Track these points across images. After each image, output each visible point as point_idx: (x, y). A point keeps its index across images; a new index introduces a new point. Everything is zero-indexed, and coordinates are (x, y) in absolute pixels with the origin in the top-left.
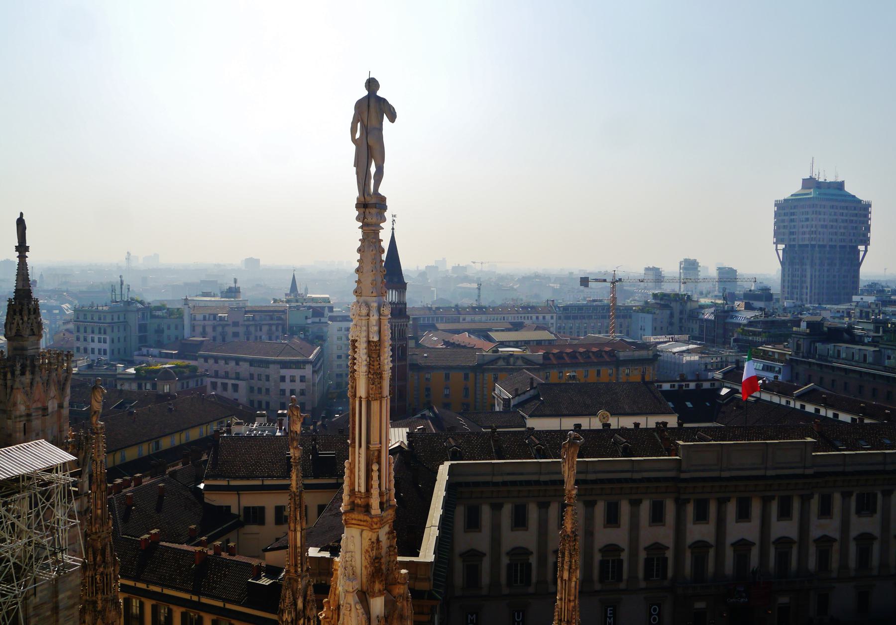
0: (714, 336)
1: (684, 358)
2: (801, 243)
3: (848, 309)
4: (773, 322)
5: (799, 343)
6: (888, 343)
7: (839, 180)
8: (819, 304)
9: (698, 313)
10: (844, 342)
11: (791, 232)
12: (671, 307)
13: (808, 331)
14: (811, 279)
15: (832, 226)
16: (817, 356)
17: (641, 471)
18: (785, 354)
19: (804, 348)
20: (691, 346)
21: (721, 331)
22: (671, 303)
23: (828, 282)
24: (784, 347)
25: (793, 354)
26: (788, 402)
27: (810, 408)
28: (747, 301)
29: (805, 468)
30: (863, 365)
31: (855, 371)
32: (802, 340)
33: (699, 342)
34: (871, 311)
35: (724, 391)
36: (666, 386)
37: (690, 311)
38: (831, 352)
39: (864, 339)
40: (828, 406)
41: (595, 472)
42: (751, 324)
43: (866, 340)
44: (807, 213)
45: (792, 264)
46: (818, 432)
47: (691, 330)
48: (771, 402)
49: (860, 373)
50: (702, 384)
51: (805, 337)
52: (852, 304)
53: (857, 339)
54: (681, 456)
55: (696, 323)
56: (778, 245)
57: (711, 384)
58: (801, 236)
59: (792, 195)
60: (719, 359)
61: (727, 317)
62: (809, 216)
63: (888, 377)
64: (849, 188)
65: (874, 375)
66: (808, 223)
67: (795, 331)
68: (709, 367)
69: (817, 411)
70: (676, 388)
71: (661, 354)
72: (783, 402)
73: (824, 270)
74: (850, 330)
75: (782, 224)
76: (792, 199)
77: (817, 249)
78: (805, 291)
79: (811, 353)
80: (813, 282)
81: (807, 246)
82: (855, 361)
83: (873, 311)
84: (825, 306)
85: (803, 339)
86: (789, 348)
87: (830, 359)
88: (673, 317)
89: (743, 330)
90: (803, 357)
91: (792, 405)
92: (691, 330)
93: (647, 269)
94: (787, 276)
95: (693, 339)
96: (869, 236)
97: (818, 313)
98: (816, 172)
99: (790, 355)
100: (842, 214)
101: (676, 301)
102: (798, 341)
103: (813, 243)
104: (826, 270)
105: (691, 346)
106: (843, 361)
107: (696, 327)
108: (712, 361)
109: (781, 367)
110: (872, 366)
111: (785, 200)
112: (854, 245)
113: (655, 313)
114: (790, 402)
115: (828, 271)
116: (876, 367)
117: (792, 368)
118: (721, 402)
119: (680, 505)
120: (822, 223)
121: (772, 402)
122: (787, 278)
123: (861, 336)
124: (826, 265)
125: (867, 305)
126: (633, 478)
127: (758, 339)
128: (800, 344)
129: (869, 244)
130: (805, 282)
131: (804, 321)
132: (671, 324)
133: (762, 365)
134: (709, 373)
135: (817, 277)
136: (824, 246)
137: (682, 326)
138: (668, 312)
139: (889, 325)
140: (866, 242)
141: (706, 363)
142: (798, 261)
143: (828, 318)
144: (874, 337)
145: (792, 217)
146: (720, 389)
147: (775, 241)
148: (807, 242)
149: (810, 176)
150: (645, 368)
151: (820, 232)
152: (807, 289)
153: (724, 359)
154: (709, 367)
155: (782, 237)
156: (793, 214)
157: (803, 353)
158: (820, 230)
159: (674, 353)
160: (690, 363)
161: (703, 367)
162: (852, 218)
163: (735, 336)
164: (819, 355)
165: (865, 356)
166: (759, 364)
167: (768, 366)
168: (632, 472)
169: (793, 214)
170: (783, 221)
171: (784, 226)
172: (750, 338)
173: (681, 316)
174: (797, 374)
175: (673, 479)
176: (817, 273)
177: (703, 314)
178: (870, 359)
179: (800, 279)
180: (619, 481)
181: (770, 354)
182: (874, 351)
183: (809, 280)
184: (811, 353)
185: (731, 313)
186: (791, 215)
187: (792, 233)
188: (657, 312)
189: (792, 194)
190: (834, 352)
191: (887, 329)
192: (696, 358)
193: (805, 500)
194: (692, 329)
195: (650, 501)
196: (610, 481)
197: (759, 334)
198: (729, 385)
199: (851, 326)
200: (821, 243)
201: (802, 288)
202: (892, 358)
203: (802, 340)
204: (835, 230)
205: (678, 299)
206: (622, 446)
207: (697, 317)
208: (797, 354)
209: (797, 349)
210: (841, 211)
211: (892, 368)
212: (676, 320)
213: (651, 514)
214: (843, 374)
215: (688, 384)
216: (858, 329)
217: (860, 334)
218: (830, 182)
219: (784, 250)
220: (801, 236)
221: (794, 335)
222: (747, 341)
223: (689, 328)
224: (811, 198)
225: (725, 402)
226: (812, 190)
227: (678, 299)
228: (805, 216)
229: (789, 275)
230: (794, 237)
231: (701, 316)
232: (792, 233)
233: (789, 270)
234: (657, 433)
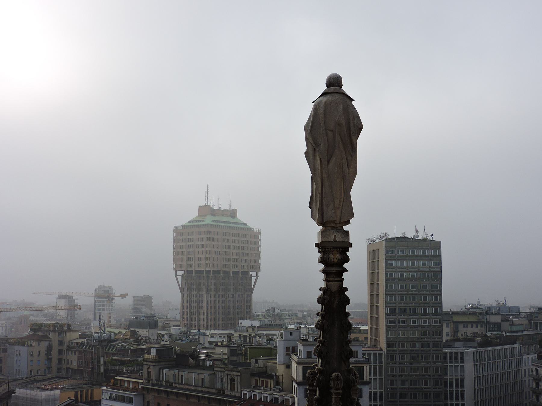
2: (197, 269)
5: (149, 370)
6: (220, 366)
12: (50, 338)
14: (207, 304)
19: (153, 376)
23: (223, 307)
37: (69, 341)
39: (206, 363)
44: (202, 239)
45: (190, 290)
51: (154, 364)
53: (201, 363)
55: (75, 354)
58: (197, 262)
59: (189, 222)
62: (203, 243)
66: (203, 249)
73: (219, 295)
75: (180, 250)
78: (202, 317)
80: (209, 307)
81: (202, 272)
83: (250, 335)
85: (152, 366)
90: (153, 385)
93: (60, 297)
96: (259, 262)
97: (197, 339)
98: (210, 200)
99: (142, 383)
100: (234, 241)
102: (149, 368)
103: (208, 269)
104: (221, 296)
111: (183, 226)
112: (246, 270)
113: (31, 345)
115: (223, 296)
120: (216, 249)
122: (185, 305)
124: (221, 290)
129: (259, 270)
130: (202, 308)
135: (213, 302)
136: (218, 272)
138: (46, 344)
140: (257, 268)
142: (195, 287)
147: (174, 267)
148: (202, 269)
149: (205, 204)
151: (214, 258)
152: (204, 315)
155: (180, 263)
156: (190, 240)
157: (152, 380)
162: (243, 245)
164: (166, 382)
170: (181, 247)
171: (182, 252)
173: (60, 348)
176: (213, 299)
179: (198, 305)
182: (210, 374)
186: (188, 242)
188: (34, 344)
194: (71, 360)
200: (215, 269)
201: (199, 314)
203: (151, 367)
204: (228, 257)
218: (225, 210)
219: (182, 276)
220: (197, 262)
223: (68, 360)
232: (189, 259)
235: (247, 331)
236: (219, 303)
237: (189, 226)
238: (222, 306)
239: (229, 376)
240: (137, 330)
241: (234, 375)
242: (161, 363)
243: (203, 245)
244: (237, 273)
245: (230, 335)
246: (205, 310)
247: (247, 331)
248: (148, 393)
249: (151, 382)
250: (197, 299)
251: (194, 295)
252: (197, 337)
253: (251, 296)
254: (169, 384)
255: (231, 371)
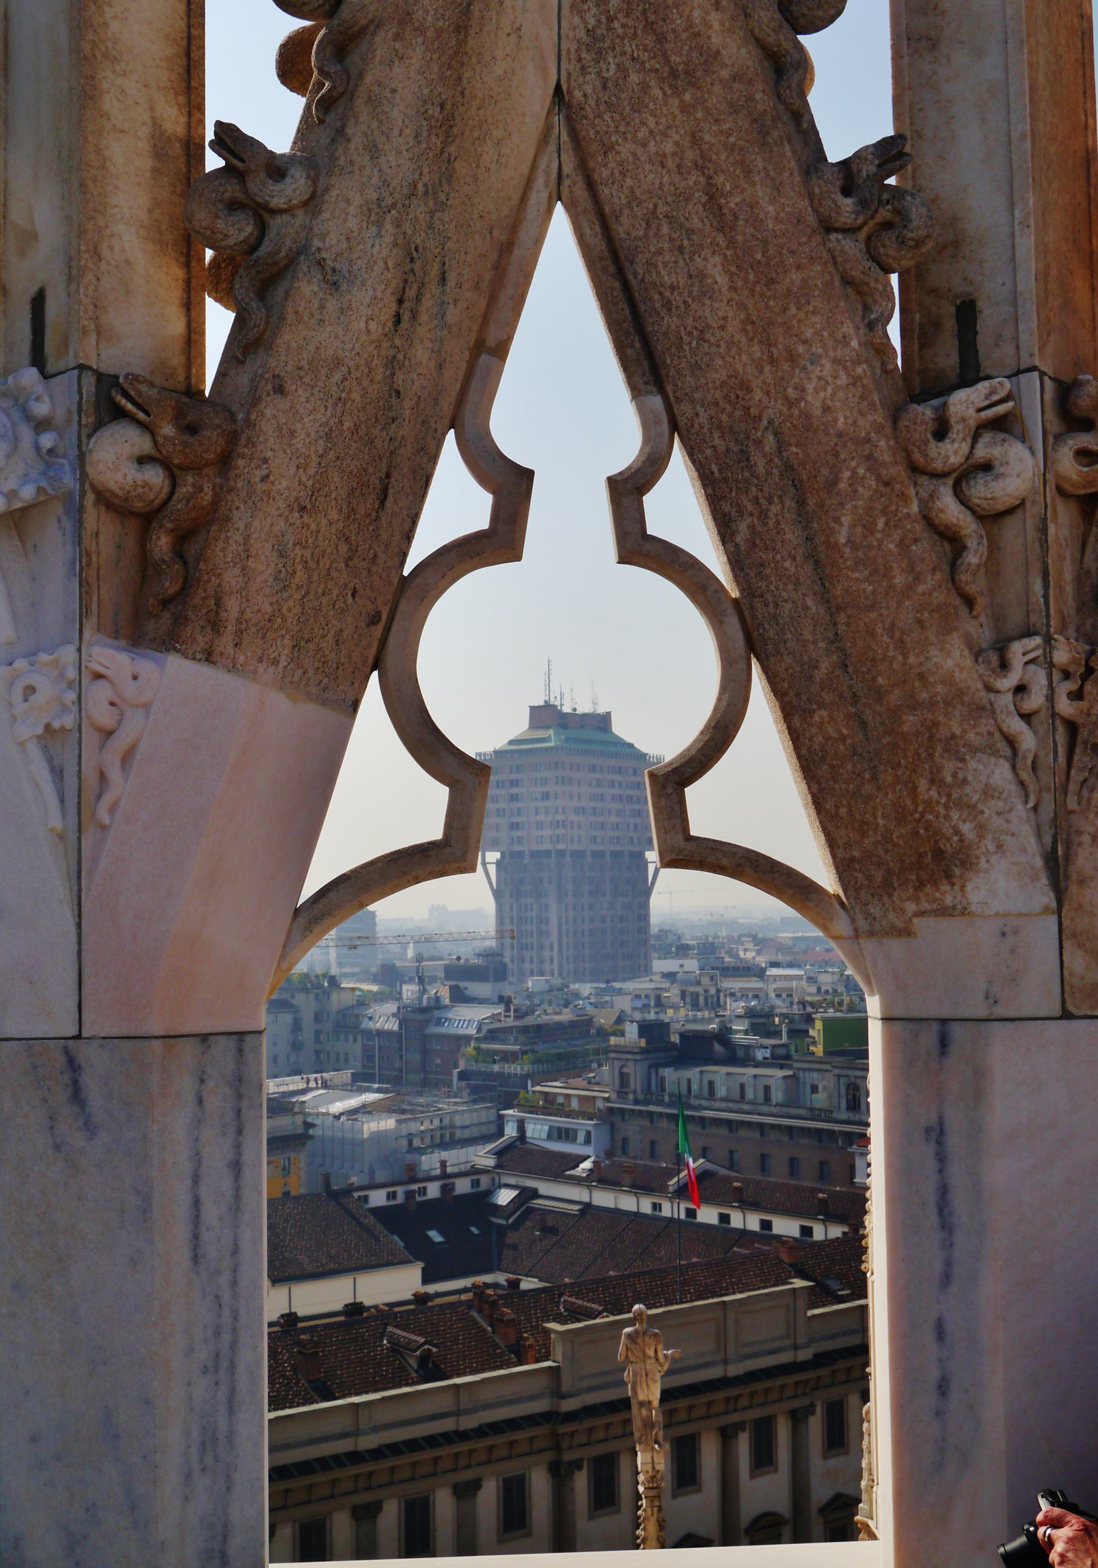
0: (400, 1070)
1: (366, 1127)
2: (535, 848)
3: (657, 989)
4: (539, 1028)
5: (625, 1070)
7: (601, 710)
8: (608, 982)
9: (357, 1016)
10: (716, 1063)
11: (513, 824)
13: (643, 1043)
14: (560, 925)
15: (595, 809)
16: (667, 1098)
17: (475, 1410)
18: (594, 1098)
20: (370, 1097)
21: (415, 1057)
22: (293, 997)
24: (589, 1083)
25: (614, 1096)
26: (656, 1207)
27: (708, 1215)
28: (453, 983)
29: (796, 1347)
30: (765, 1109)
31: (749, 1124)
32: (631, 1064)
33: (376, 1086)
34: (702, 992)
35: (505, 1197)
36: (378, 1198)
37: (338, 1012)
38: (695, 1087)
40: (747, 1204)
41: (375, 1429)
42: (493, 1035)
43: (760, 1055)
45: (517, 894)
46: (791, 1265)
47: (342, 1057)
48: (617, 1212)
49: (761, 1126)
50: (453, 1184)
51: (637, 1057)
52: (653, 978)
53: (740, 1053)
54: (559, 1358)
55: (355, 1040)
56: (487, 853)
57: (472, 1181)
59: (511, 742)
60: (436, 1122)
61: (427, 1021)
62: (549, 789)
63: (819, 1131)
64: (620, 729)
65: (790, 1129)
67: (616, 1046)
68: (417, 1143)
69: (725, 1218)
70: (400, 1199)
71: (316, 1122)
72: (646, 1207)
74: (723, 1036)
76: (512, 752)
77: (568, 859)
78: (547, 954)
79: (653, 1092)
80: (564, 932)
81: (547, 853)
82: (748, 1103)
83: (706, 991)
84: (617, 985)
86: (598, 1084)
87: (697, 1102)
88: (301, 1030)
89: (477, 1049)
90: (636, 1102)
91: (667, 1211)
92: (342, 1057)
94: (507, 920)
95: (360, 1080)
98: (555, 692)
99: (607, 1100)
101: (305, 990)
102: (622, 1066)
103: (560, 847)
105: (370, 1097)
106: (724, 1105)
107: (355, 1049)
108: (422, 1128)
109: (591, 1128)
110: (785, 1110)
111: (496, 752)
112: (636, 849)
114: (660, 1205)
116: (794, 1111)
117: (612, 1126)
118: (503, 1222)
119: (560, 1473)
121: (620, 1210)
122: (508, 927)
123: (747, 1048)
125: (693, 979)
126: (461, 1428)
127: (515, 1069)
128: (628, 1074)
130: (547, 934)
131: (632, 1022)
132: (296, 1046)
133: (546, 1128)
134: (423, 1158)
136: (578, 854)
137: (321, 1052)
139: (777, 1020)
141: (410, 1134)
143: (628, 1011)
144: (774, 1046)
145: (515, 791)
146: (489, 1193)
148: (547, 846)
149: (546, 702)
150: (289, 1159)
153: (446, 1122)
154: (417, 1143)
157: (635, 1092)
158: (573, 818)
159: (337, 1117)
160: (379, 1137)
161: (404, 1143)
162: (630, 792)
163: (462, 1065)
165: (767, 1089)
166: (539, 1127)
167: (559, 1129)
168: (457, 1413)
169: (514, 783)
171: (498, 810)
172: (496, 1068)
174: (625, 1141)
175: (547, 1417)
176: (571, 914)
177: (370, 1018)
178: (777, 1096)
180: (432, 1441)
181: (560, 1100)
182: (785, 1077)
183: (554, 930)
184: (653, 1092)
185: (437, 1014)
187: (514, 826)
189: (512, 738)
190: (701, 1085)
191: (772, 1028)
192: (388, 1123)
193: (798, 1418)
194: (346, 1054)
195: (498, 1481)
196: (413, 1445)
197: (508, 1057)
198: (512, 1181)
199: (726, 1028)
200: (576, 847)
201: (541, 947)
202: (820, 1088)
204: (600, 819)
205: (309, 986)
206: (418, 1353)
207: (357, 1027)
208: (622, 1094)
209: (622, 1086)
210: (611, 777)
211: (826, 1111)
212: (307, 1035)
213: (501, 1512)
214: (724, 1131)
215: (425, 1188)
216: (738, 1032)
217: (745, 1042)
218: (584, 715)
219: (498, 864)
221: (612, 1055)
222: (490, 1076)
223: (338, 1054)
224: (551, 748)
225: (511, 1220)
226: (551, 732)
227: (309, 986)
228: (541, 789)
229: (512, 919)
230: (519, 833)
231: (366, 1025)
232: (514, 826)
233: (512, 910)
234: (480, 1311)
235: (698, 983)
236: (583, 922)
237: (506, 752)
238: (590, 931)
239: (843, 1081)
240: (462, 984)
241: (856, 1077)
242: (652, 1055)
243: (547, 793)
244: (602, 853)
245: (658, 992)
246: (554, 938)
247: (698, 983)
248: (623, 1119)
249: (631, 1097)
250: (534, 914)
251: (526, 906)
252: (608, 998)
253: (645, 905)
254: (679, 1100)
255: (849, 1068)
